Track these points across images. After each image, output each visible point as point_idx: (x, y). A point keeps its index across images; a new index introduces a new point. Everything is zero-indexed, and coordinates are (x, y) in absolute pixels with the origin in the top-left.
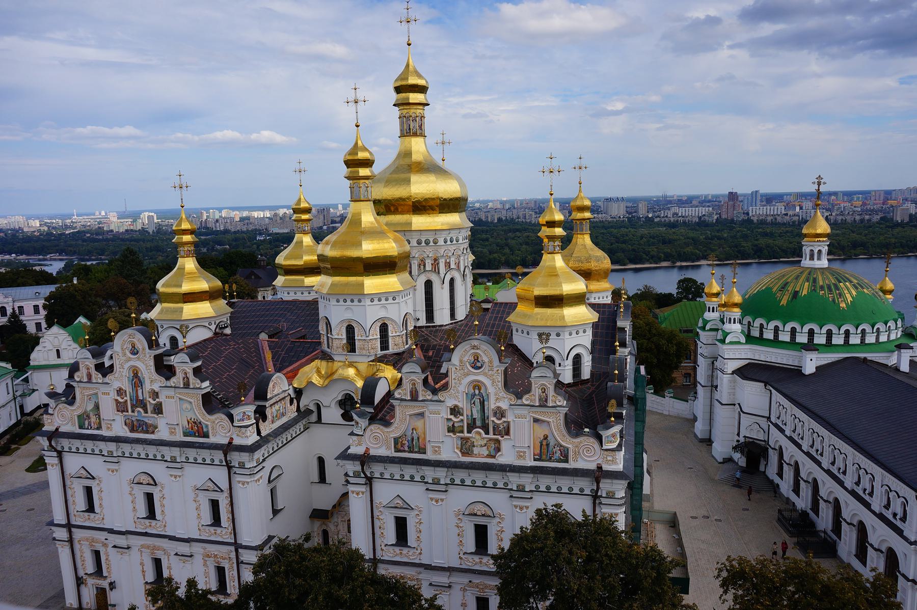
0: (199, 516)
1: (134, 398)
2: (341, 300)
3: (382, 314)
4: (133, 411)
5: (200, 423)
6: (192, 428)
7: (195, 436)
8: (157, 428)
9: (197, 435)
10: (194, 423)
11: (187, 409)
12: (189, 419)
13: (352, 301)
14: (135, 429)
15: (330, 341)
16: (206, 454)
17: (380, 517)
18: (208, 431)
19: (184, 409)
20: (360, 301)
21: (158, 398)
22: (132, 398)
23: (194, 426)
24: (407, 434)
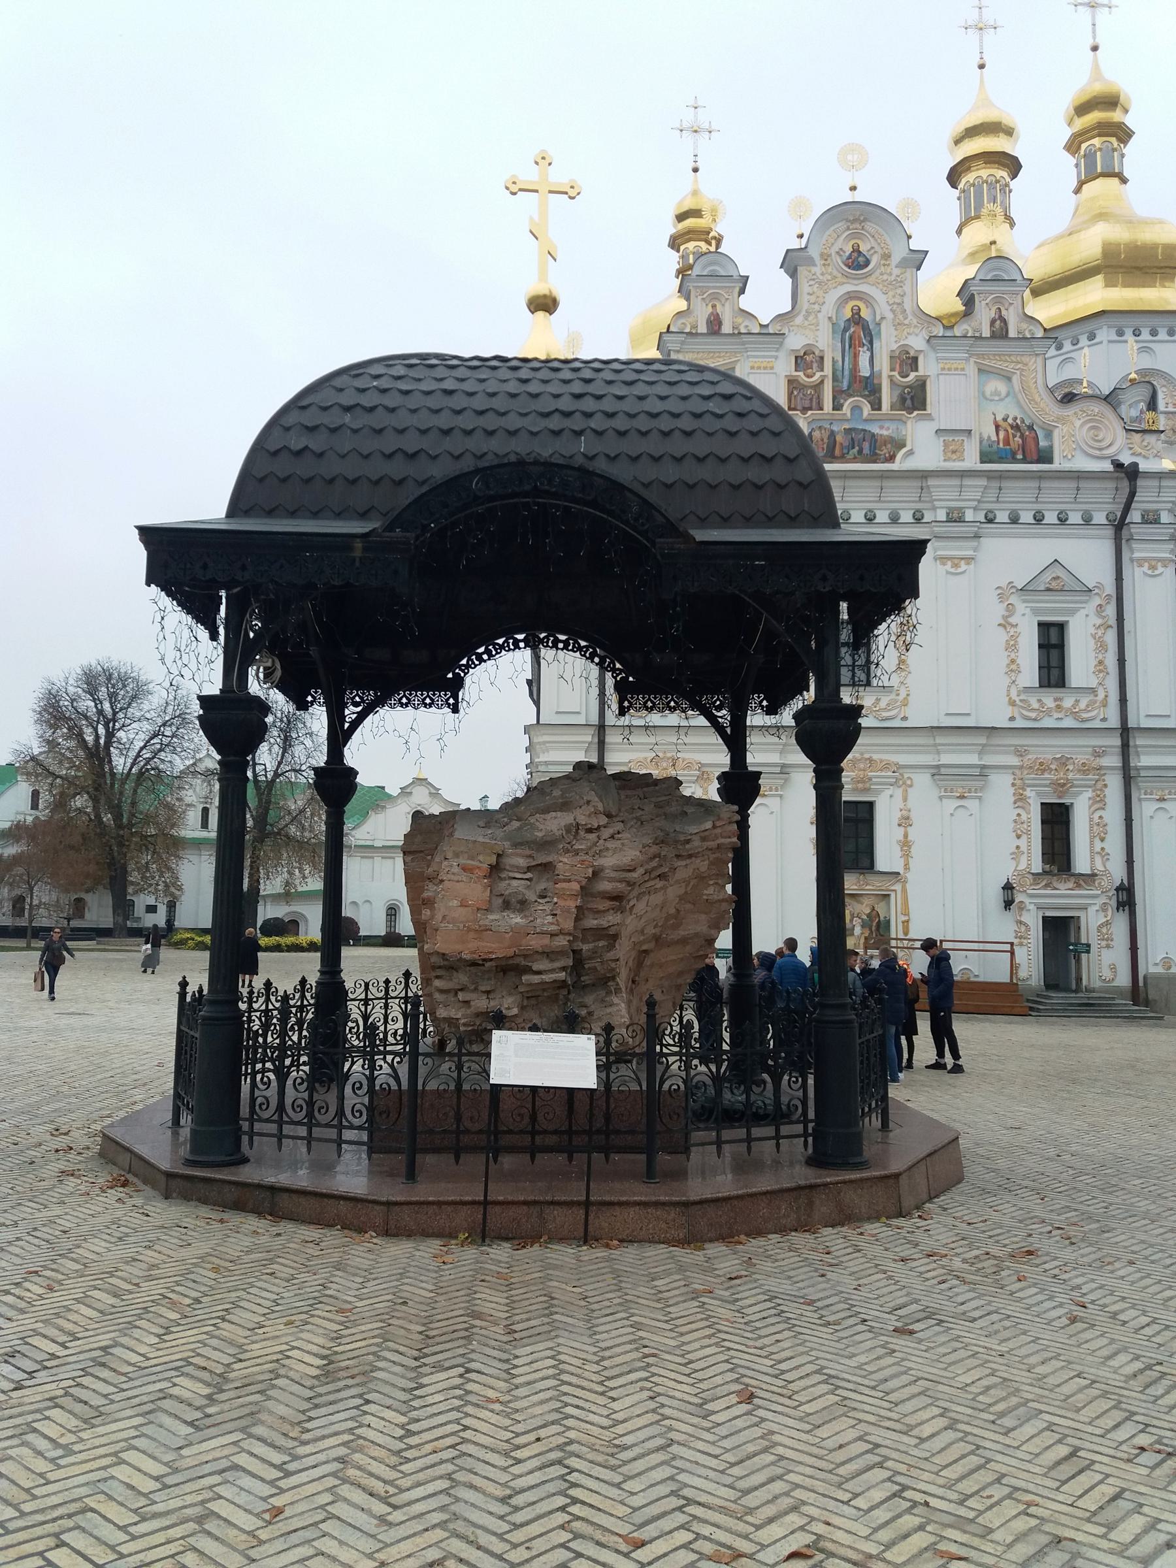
0: (1013, 667)
1: (847, 373)
4: (837, 407)
5: (1031, 428)
6: (1007, 442)
7: (1014, 460)
8: (904, 446)
9: (1020, 456)
10: (1012, 427)
11: (997, 393)
12: (999, 418)
14: (837, 452)
16: (1055, 498)
18: (1051, 447)
19: (988, 394)
21: (917, 370)
22: (839, 374)
23: (1014, 436)
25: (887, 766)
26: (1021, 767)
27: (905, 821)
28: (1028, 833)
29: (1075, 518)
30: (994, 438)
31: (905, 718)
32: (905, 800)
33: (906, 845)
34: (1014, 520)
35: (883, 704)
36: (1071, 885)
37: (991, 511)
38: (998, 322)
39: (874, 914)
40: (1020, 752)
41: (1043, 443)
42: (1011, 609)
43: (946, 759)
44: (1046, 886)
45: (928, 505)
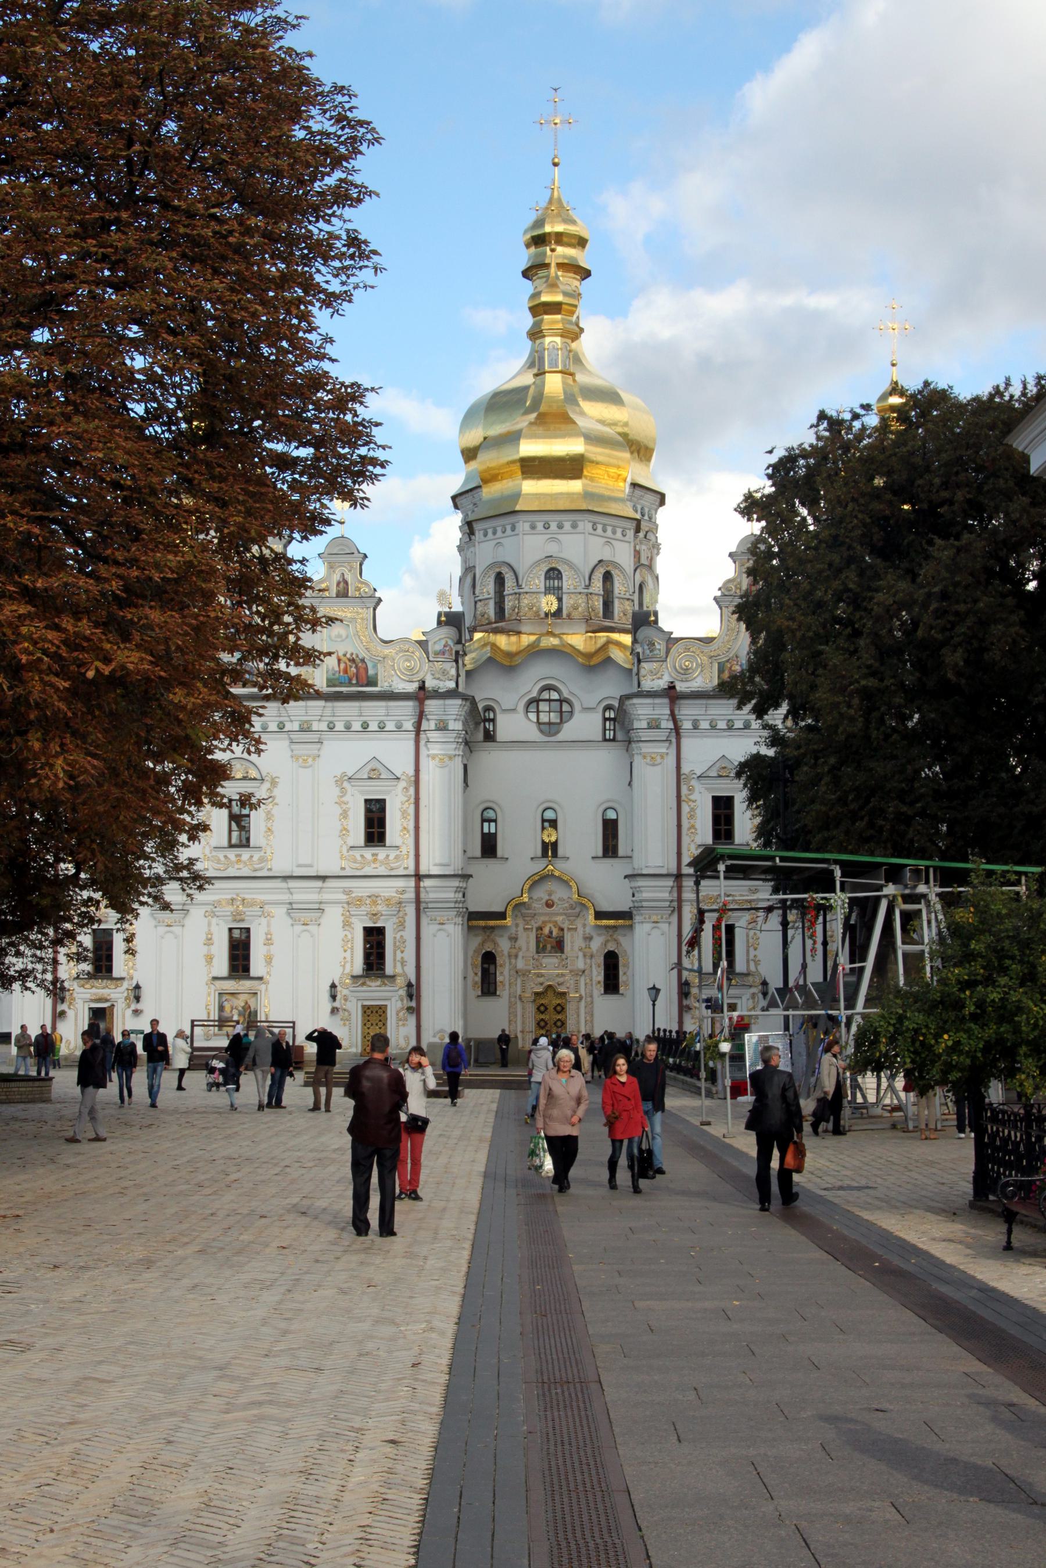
0: (344, 831)
2: (540, 526)
3: (606, 554)
5: (363, 661)
6: (346, 671)
7: (350, 684)
9: (354, 682)
10: (349, 660)
11: (339, 636)
13: (560, 526)
15: (508, 604)
16: (375, 710)
17: (692, 797)
18: (377, 674)
20: (574, 526)
24: (740, 654)
25: (252, 904)
26: (348, 903)
27: (268, 941)
28: (352, 948)
29: (390, 726)
30: (337, 669)
31: (270, 870)
32: (269, 925)
33: (269, 960)
34: (348, 727)
35: (256, 858)
36: (379, 983)
37: (331, 722)
38: (342, 585)
39: (247, 1007)
40: (347, 892)
41: (371, 672)
42: (343, 792)
43: (297, 897)
44: (363, 984)
45: (287, 719)
